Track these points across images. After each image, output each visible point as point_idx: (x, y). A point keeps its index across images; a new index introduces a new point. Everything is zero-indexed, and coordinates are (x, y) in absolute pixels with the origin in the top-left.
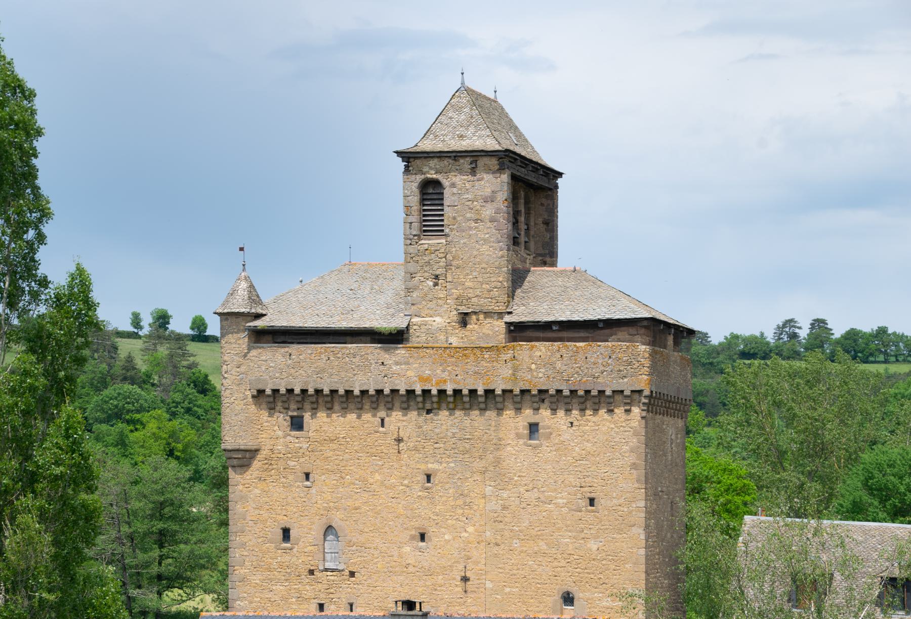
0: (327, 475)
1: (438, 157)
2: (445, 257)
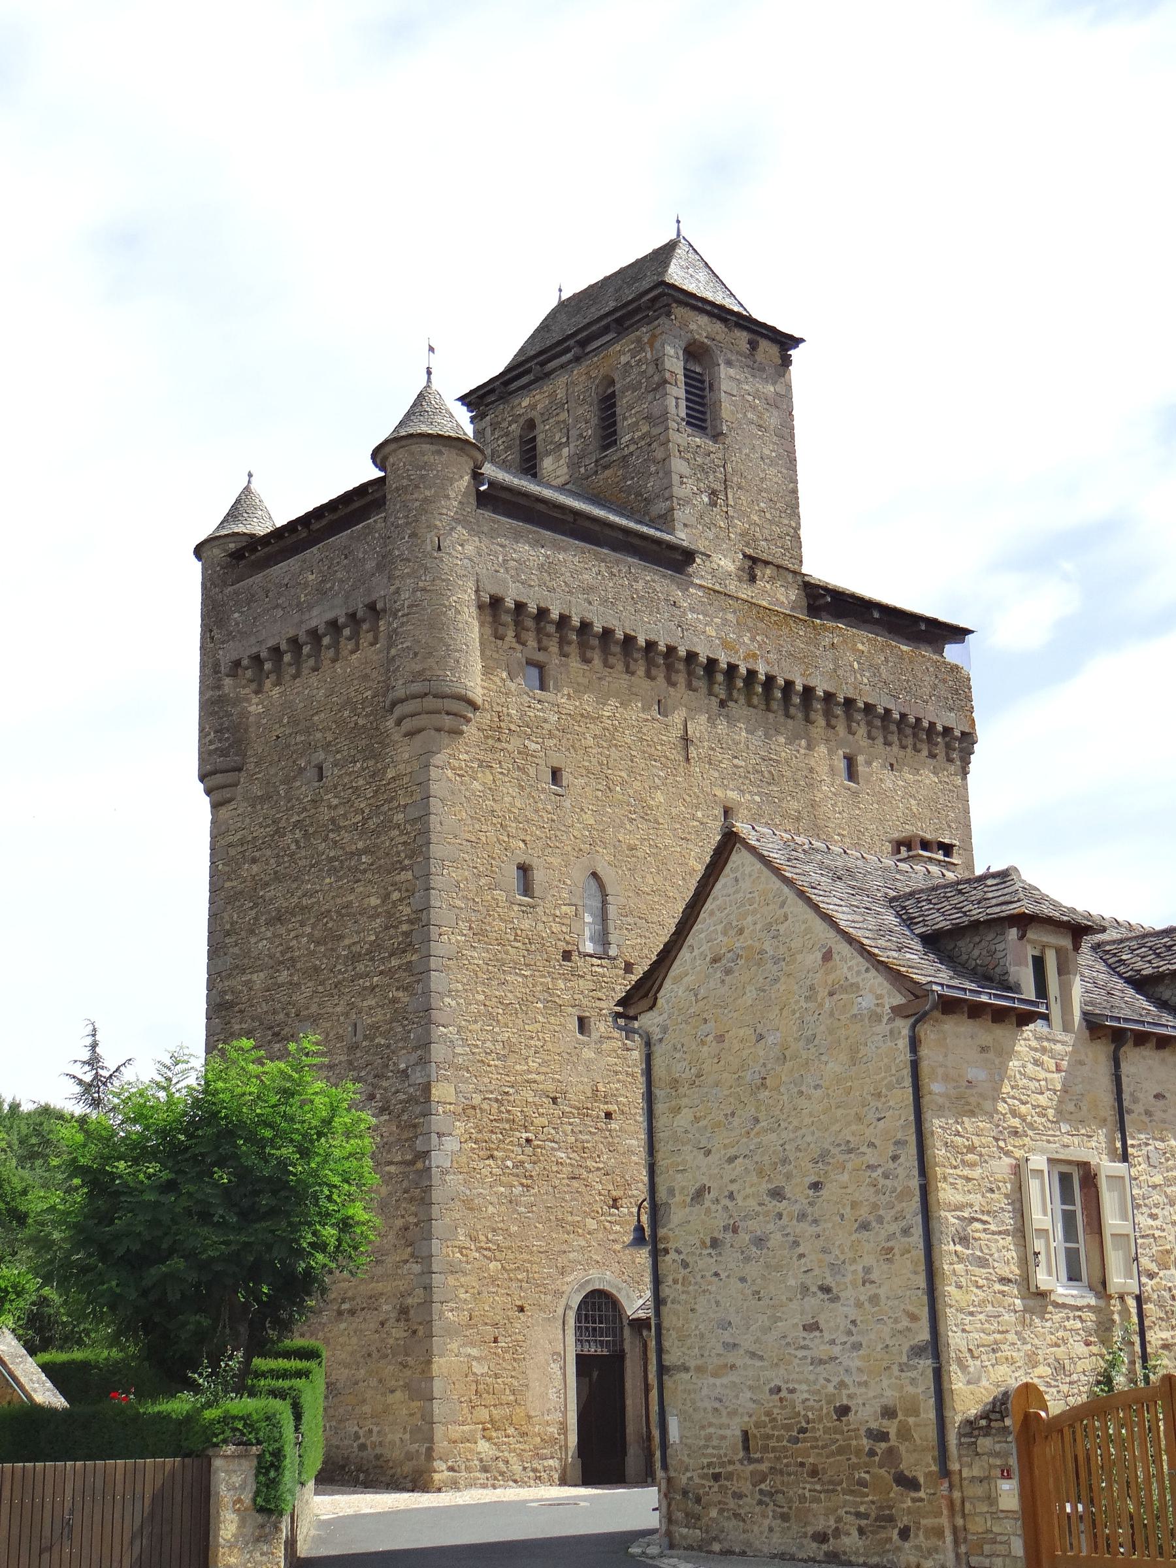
0: (587, 779)
1: (710, 314)
2: (724, 467)
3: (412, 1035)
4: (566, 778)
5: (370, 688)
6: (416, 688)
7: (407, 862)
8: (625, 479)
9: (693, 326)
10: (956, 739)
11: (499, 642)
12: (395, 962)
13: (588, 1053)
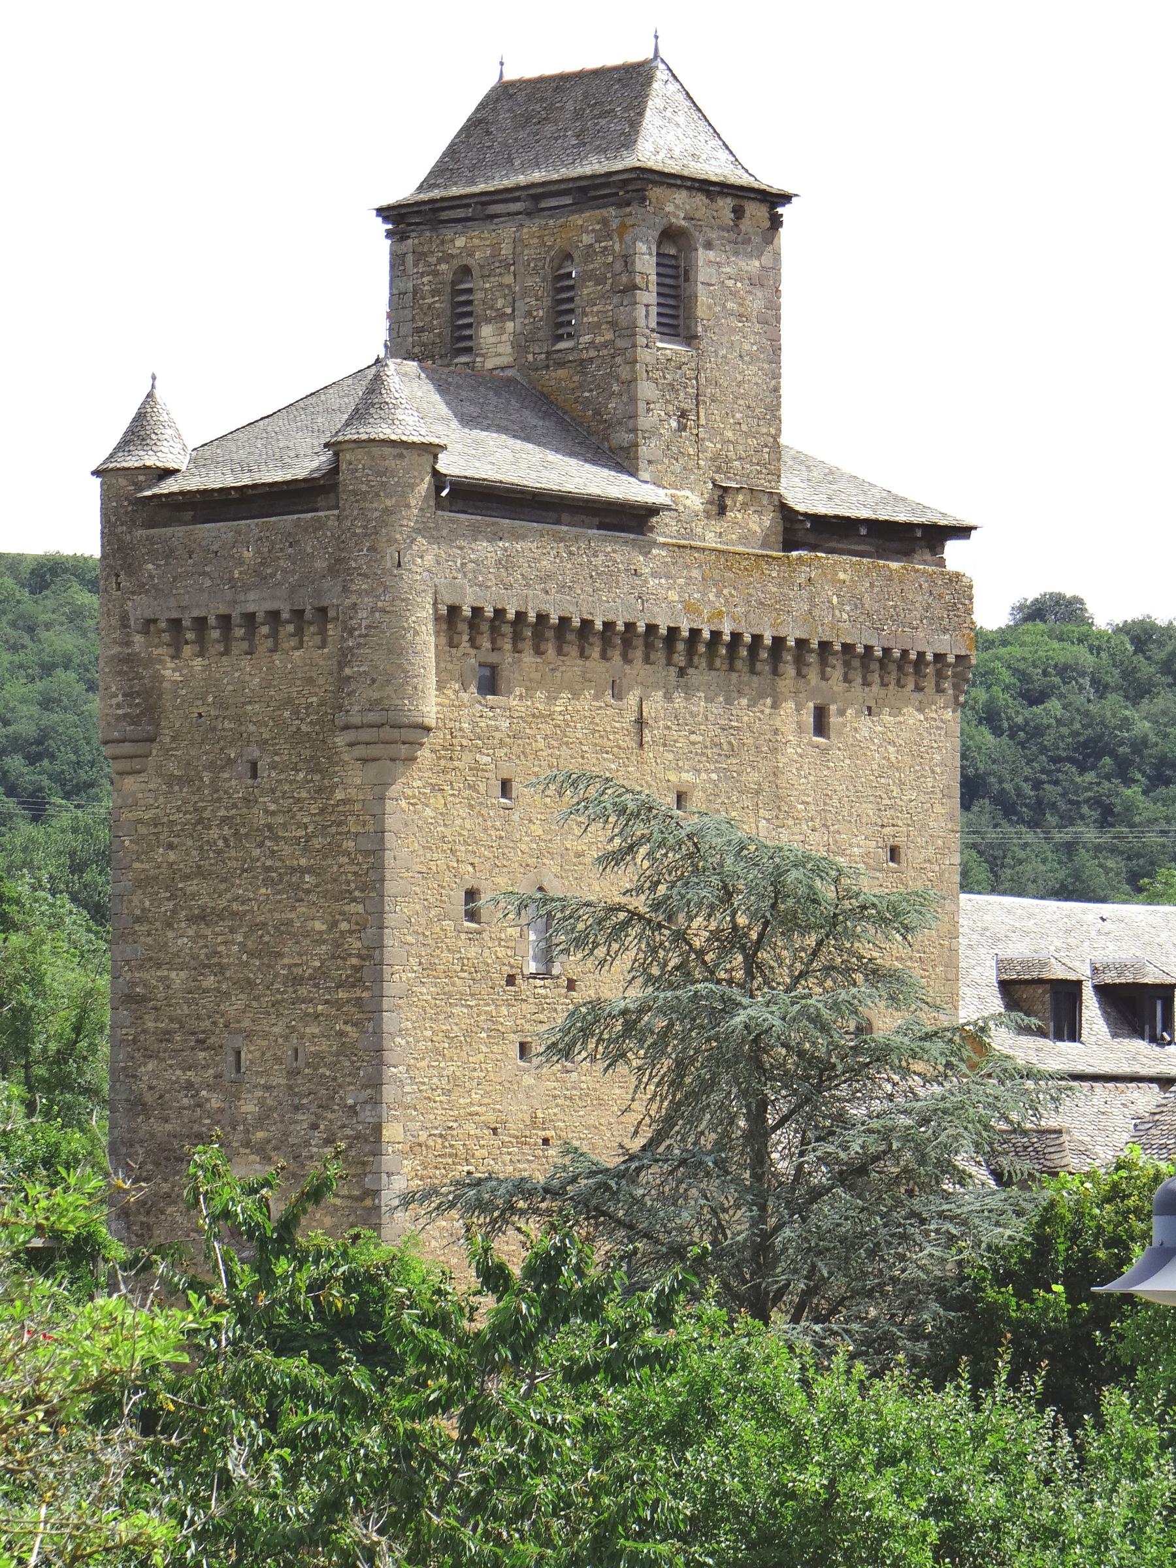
1: (688, 188)
3: (362, 1073)
4: (517, 788)
5: (316, 694)
6: (372, 717)
7: (357, 894)
8: (581, 387)
9: (669, 208)
10: (949, 665)
11: (454, 651)
12: (342, 994)
13: (528, 1080)
